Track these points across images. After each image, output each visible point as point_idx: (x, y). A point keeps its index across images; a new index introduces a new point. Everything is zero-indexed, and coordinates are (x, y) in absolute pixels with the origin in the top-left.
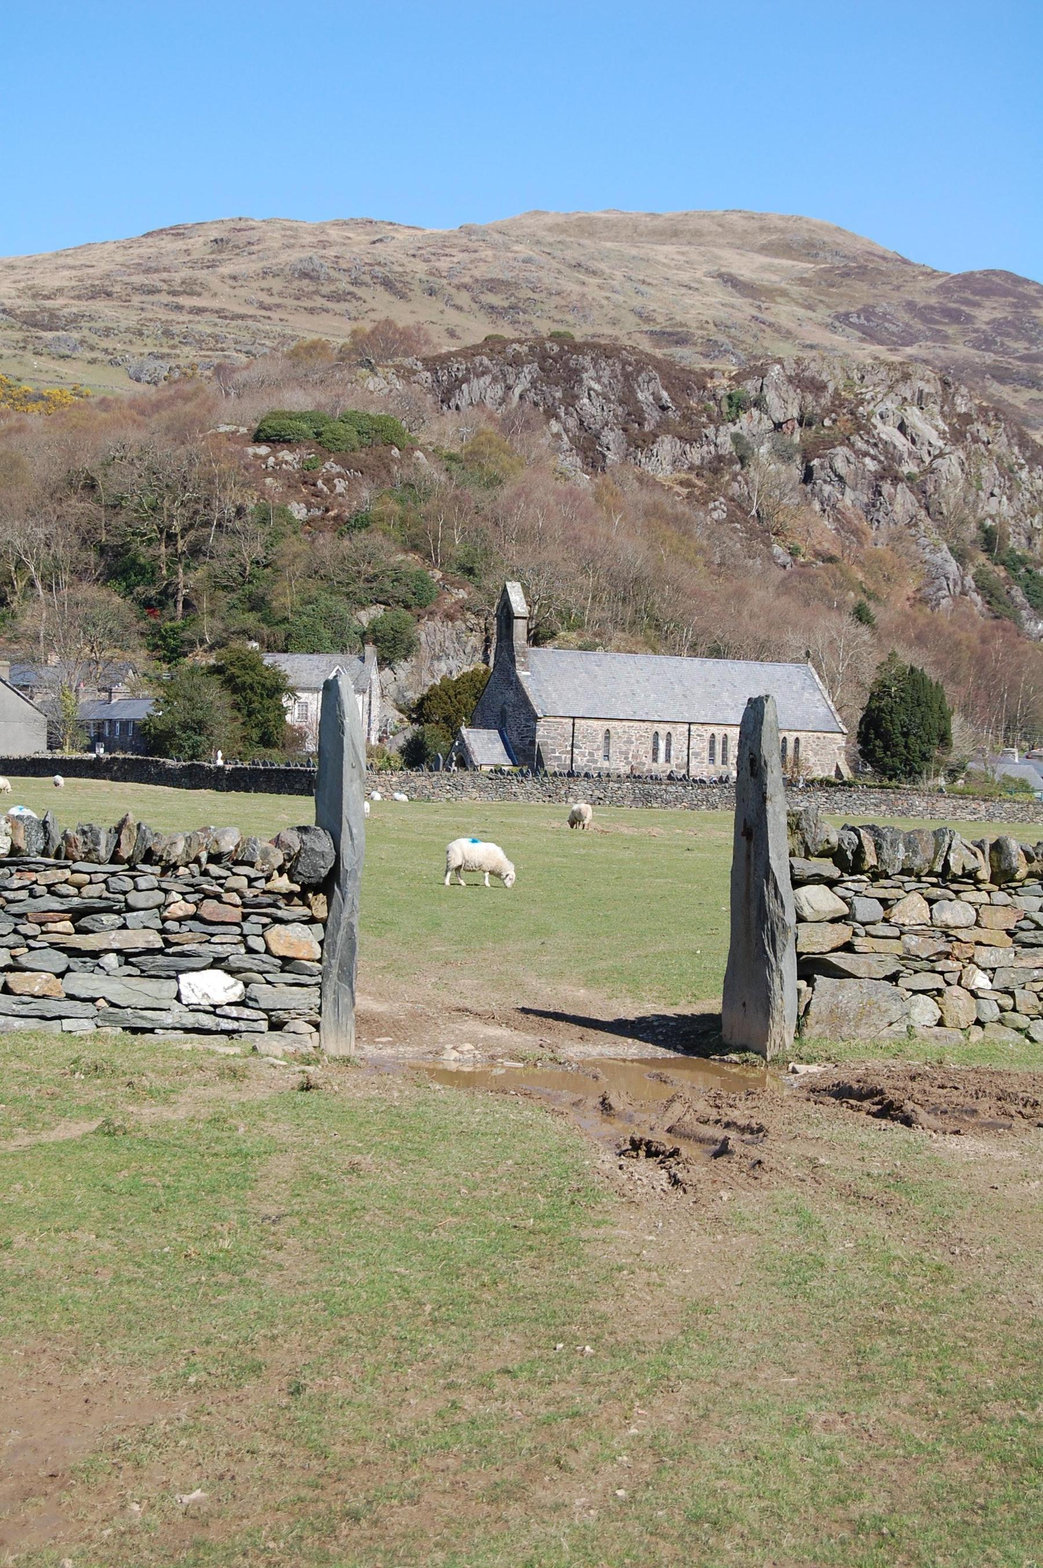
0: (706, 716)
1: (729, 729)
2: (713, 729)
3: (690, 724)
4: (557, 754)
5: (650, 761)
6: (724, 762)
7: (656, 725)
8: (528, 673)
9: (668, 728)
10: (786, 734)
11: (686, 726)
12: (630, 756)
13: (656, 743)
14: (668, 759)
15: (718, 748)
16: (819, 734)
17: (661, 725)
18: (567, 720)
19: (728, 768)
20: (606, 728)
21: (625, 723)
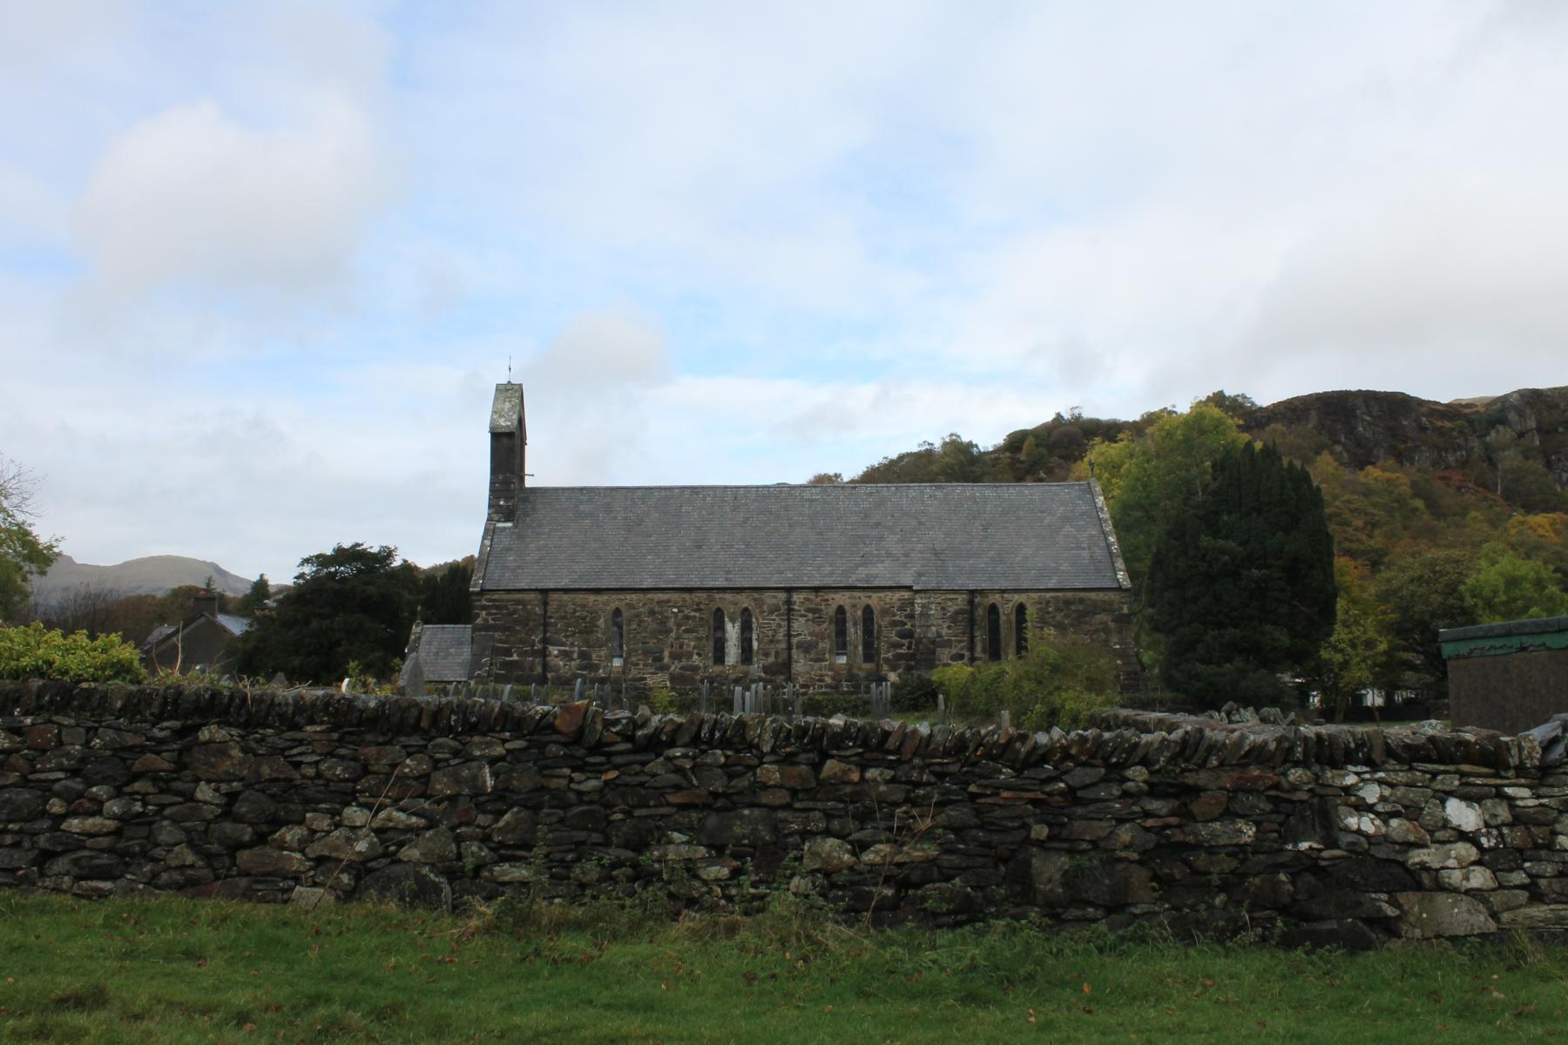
0: (831, 574)
1: (874, 595)
2: (841, 599)
3: (789, 590)
4: (515, 657)
5: (711, 662)
6: (868, 657)
7: (717, 596)
8: (510, 524)
9: (745, 601)
10: (996, 598)
11: (782, 596)
12: (666, 654)
13: (720, 627)
14: (747, 654)
15: (854, 633)
16: (1069, 595)
17: (728, 596)
18: (532, 596)
19: (878, 666)
20: (613, 606)
21: (649, 596)
